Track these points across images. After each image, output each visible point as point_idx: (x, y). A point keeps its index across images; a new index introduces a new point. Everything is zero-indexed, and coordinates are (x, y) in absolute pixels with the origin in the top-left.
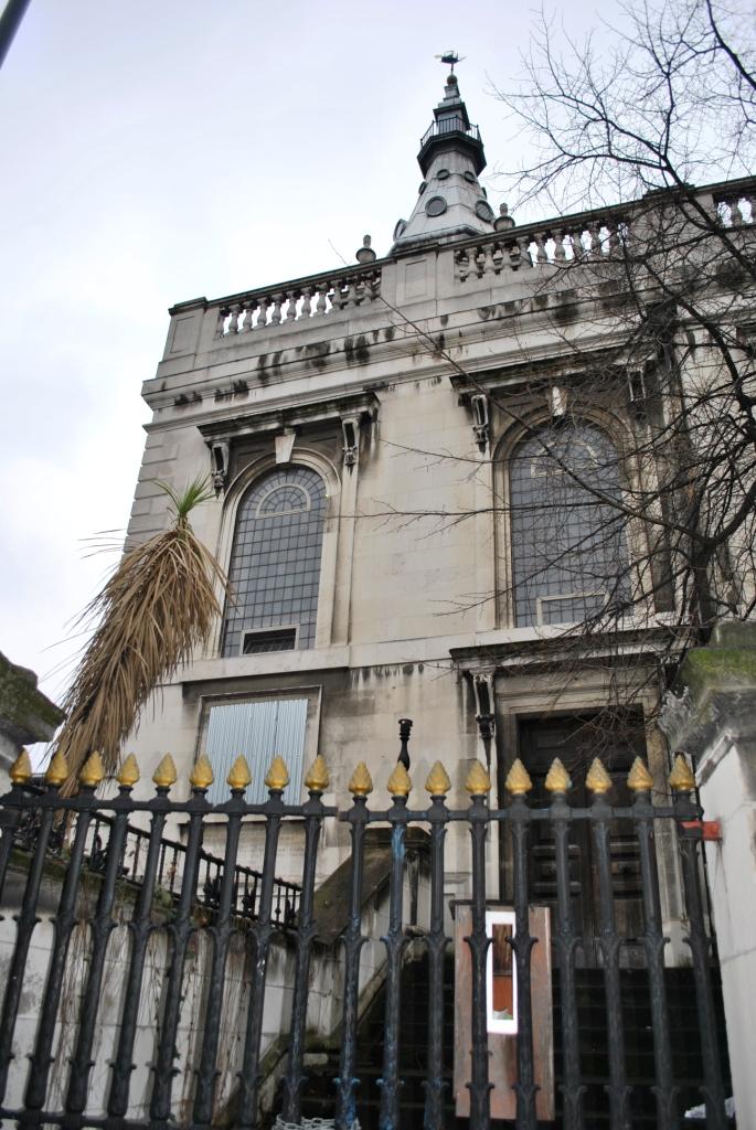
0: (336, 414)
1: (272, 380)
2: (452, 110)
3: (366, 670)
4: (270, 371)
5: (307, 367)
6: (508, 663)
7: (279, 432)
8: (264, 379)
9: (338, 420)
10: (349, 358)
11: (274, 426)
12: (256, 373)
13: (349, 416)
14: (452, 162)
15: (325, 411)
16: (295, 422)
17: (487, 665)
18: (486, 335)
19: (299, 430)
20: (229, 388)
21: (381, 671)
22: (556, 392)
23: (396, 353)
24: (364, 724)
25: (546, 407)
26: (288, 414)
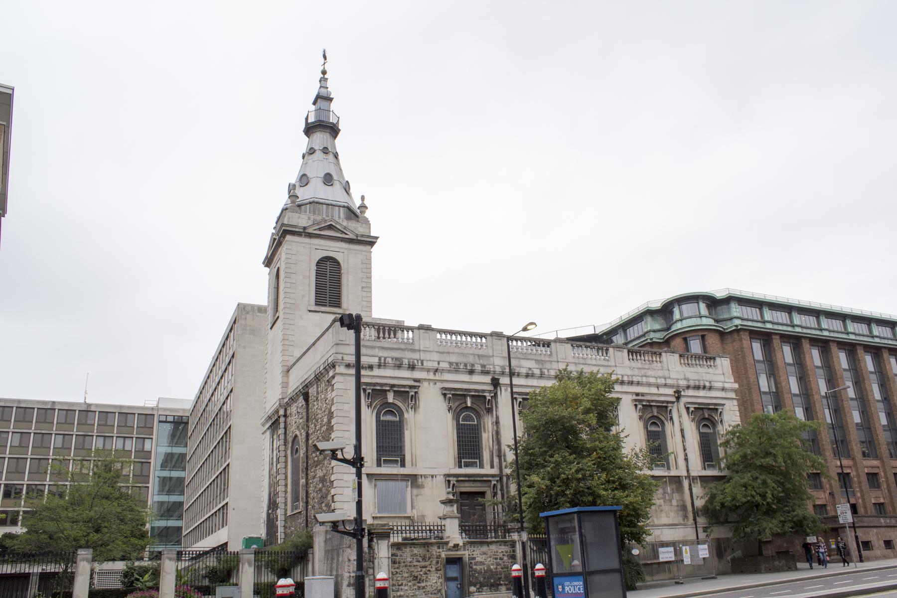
0: (408, 390)
1: (382, 367)
2: (323, 98)
3: (421, 476)
4: (383, 364)
5: (395, 366)
6: (460, 479)
7: (389, 391)
8: (379, 366)
9: (408, 392)
10: (409, 368)
11: (388, 388)
12: (378, 364)
13: (412, 392)
14: (320, 139)
15: (405, 388)
16: (395, 389)
17: (455, 479)
18: (449, 371)
19: (395, 392)
20: (367, 366)
21: (426, 476)
22: (468, 398)
23: (422, 369)
24: (422, 491)
25: (466, 402)
26: (393, 386)
